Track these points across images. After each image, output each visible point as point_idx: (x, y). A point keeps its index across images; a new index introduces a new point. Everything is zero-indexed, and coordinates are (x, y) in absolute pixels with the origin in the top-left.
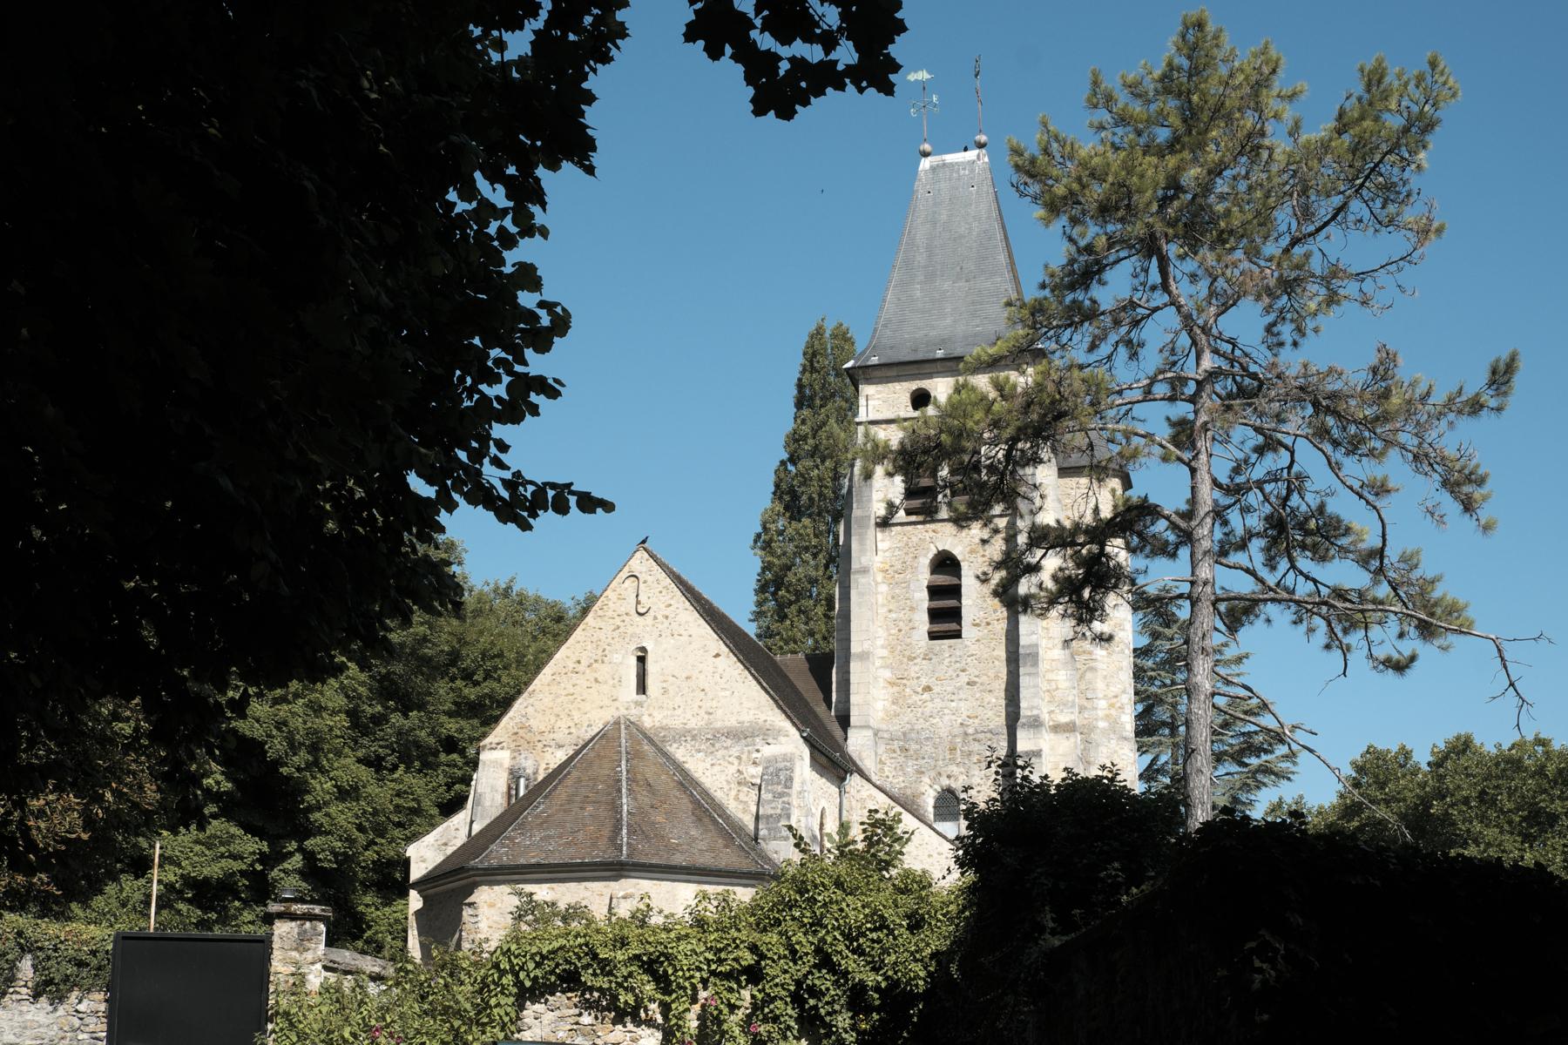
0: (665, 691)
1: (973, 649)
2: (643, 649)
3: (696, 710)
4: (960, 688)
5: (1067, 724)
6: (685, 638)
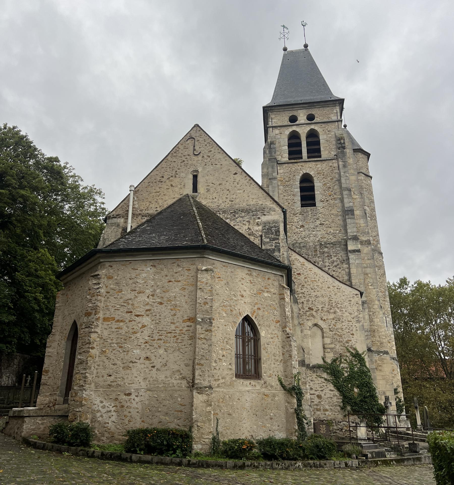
0: (208, 190)
1: (321, 210)
3: (225, 199)
5: (366, 241)
6: (218, 166)
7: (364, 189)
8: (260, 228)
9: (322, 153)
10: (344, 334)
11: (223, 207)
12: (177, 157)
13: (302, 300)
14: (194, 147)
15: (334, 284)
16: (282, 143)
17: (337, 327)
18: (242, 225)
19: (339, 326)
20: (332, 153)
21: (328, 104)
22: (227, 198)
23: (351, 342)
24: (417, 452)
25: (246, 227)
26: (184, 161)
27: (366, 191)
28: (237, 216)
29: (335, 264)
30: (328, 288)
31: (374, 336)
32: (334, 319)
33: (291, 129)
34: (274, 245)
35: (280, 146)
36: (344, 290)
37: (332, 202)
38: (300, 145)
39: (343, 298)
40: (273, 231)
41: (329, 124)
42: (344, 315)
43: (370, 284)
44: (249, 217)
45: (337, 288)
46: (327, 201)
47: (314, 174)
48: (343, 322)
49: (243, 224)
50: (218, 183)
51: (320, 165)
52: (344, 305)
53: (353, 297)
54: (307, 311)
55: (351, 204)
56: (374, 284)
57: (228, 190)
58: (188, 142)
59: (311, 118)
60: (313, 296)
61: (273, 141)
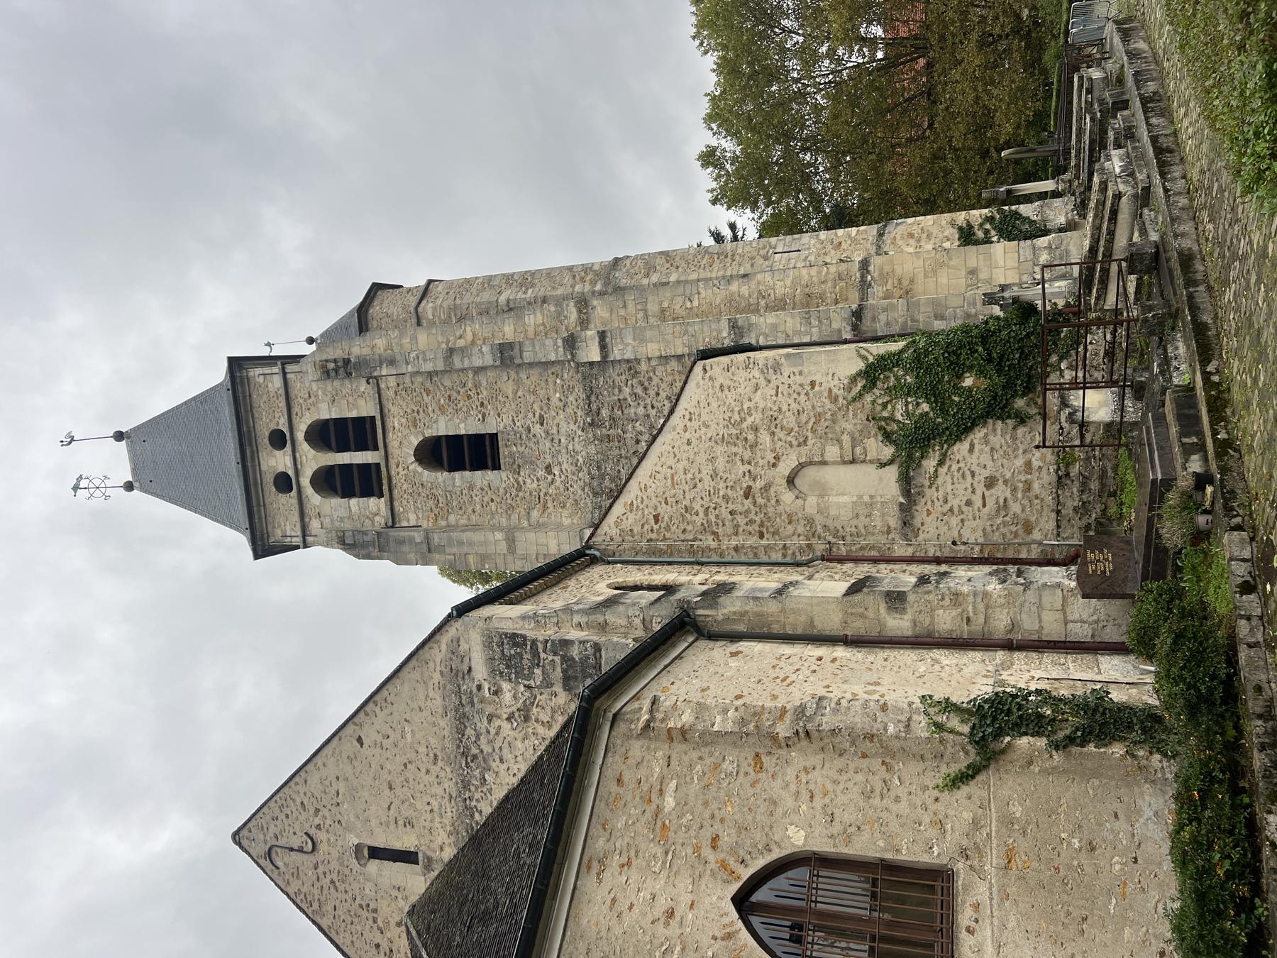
0: (409, 823)
1: (507, 420)
2: (358, 848)
3: (432, 778)
4: (547, 433)
5: (580, 311)
6: (342, 787)
7: (458, 302)
8: (506, 686)
9: (364, 414)
10: (813, 407)
11: (452, 784)
12: (323, 899)
13: (725, 513)
14: (292, 850)
15: (680, 429)
16: (344, 513)
17: (793, 424)
18: (500, 739)
19: (790, 421)
20: (362, 389)
21: (244, 397)
22: (428, 772)
23: (835, 390)
24: (1157, 253)
25: (506, 726)
26: (332, 882)
27: (461, 298)
28: (475, 751)
29: (639, 390)
30: (689, 443)
31: (822, 297)
32: (773, 434)
33: (309, 491)
34: (550, 658)
35: (350, 517)
36: (694, 403)
37: (485, 393)
38: (347, 468)
39: (714, 405)
40: (513, 652)
41: (292, 395)
42: (761, 406)
43: (688, 305)
44: (477, 716)
45: (690, 420)
46: (482, 404)
47: (416, 437)
48: (780, 409)
49: (497, 734)
50: (387, 791)
51: (395, 422)
52: (733, 404)
53: (711, 378)
54: (755, 503)
55: (485, 349)
56: (688, 292)
57: (405, 765)
58: (280, 864)
59: (278, 440)
60: (712, 484)
61: (338, 537)
